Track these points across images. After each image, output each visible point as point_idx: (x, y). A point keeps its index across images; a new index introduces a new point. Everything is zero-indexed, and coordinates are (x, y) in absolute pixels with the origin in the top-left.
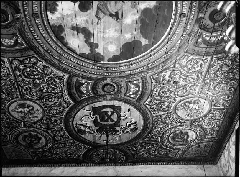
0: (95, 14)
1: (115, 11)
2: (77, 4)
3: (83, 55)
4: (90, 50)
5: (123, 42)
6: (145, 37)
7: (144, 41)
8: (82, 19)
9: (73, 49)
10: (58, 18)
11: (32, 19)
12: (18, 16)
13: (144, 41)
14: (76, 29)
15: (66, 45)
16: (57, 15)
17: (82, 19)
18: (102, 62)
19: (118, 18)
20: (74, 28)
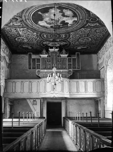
0: (60, 20)
1: (53, 21)
2: (66, 22)
3: (66, 9)
4: (63, 11)
5: (49, 13)
6: (40, 14)
7: (40, 13)
8: (65, 19)
9: (70, 11)
10: (73, 19)
11: (83, 19)
12: (88, 20)
13: (40, 13)
14: (67, 16)
15: (73, 12)
16: (73, 20)
17: (65, 19)
18: (58, 6)
19: (51, 19)
20: (69, 17)
